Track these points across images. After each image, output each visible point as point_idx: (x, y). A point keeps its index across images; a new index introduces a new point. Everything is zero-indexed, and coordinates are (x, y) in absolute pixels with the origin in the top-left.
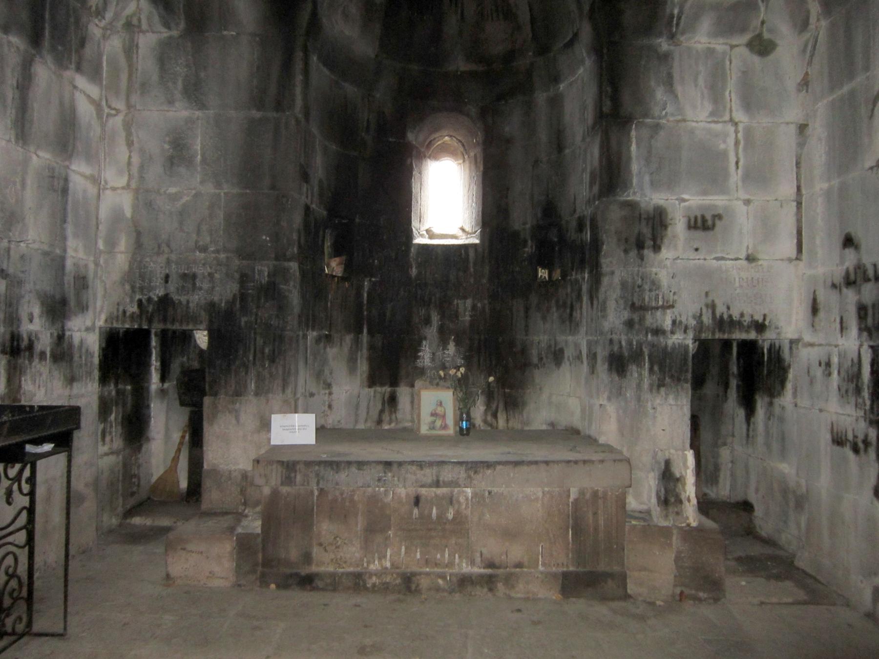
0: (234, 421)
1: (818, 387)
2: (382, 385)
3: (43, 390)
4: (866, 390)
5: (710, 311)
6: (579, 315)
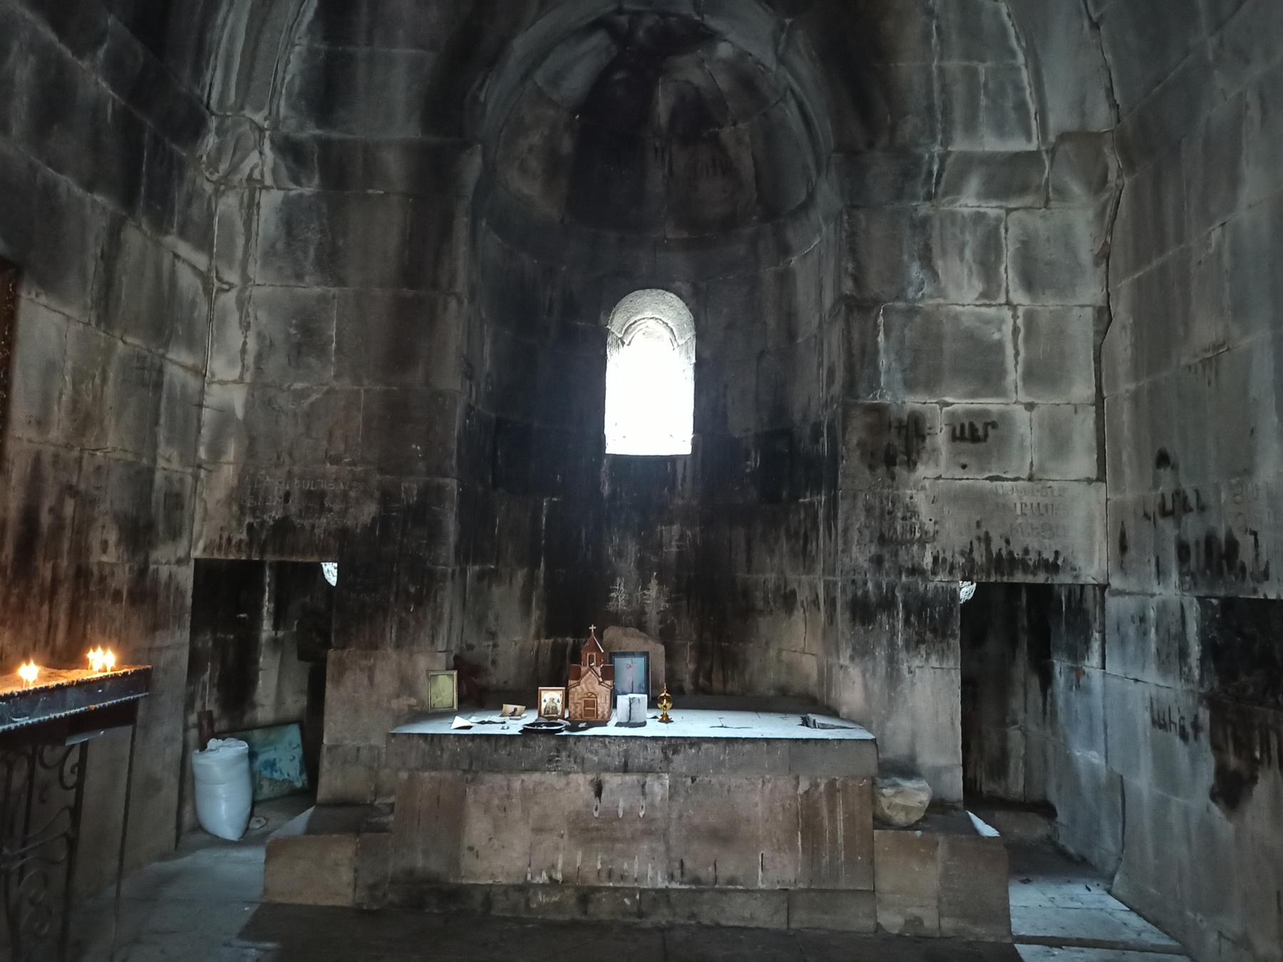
5: (983, 545)
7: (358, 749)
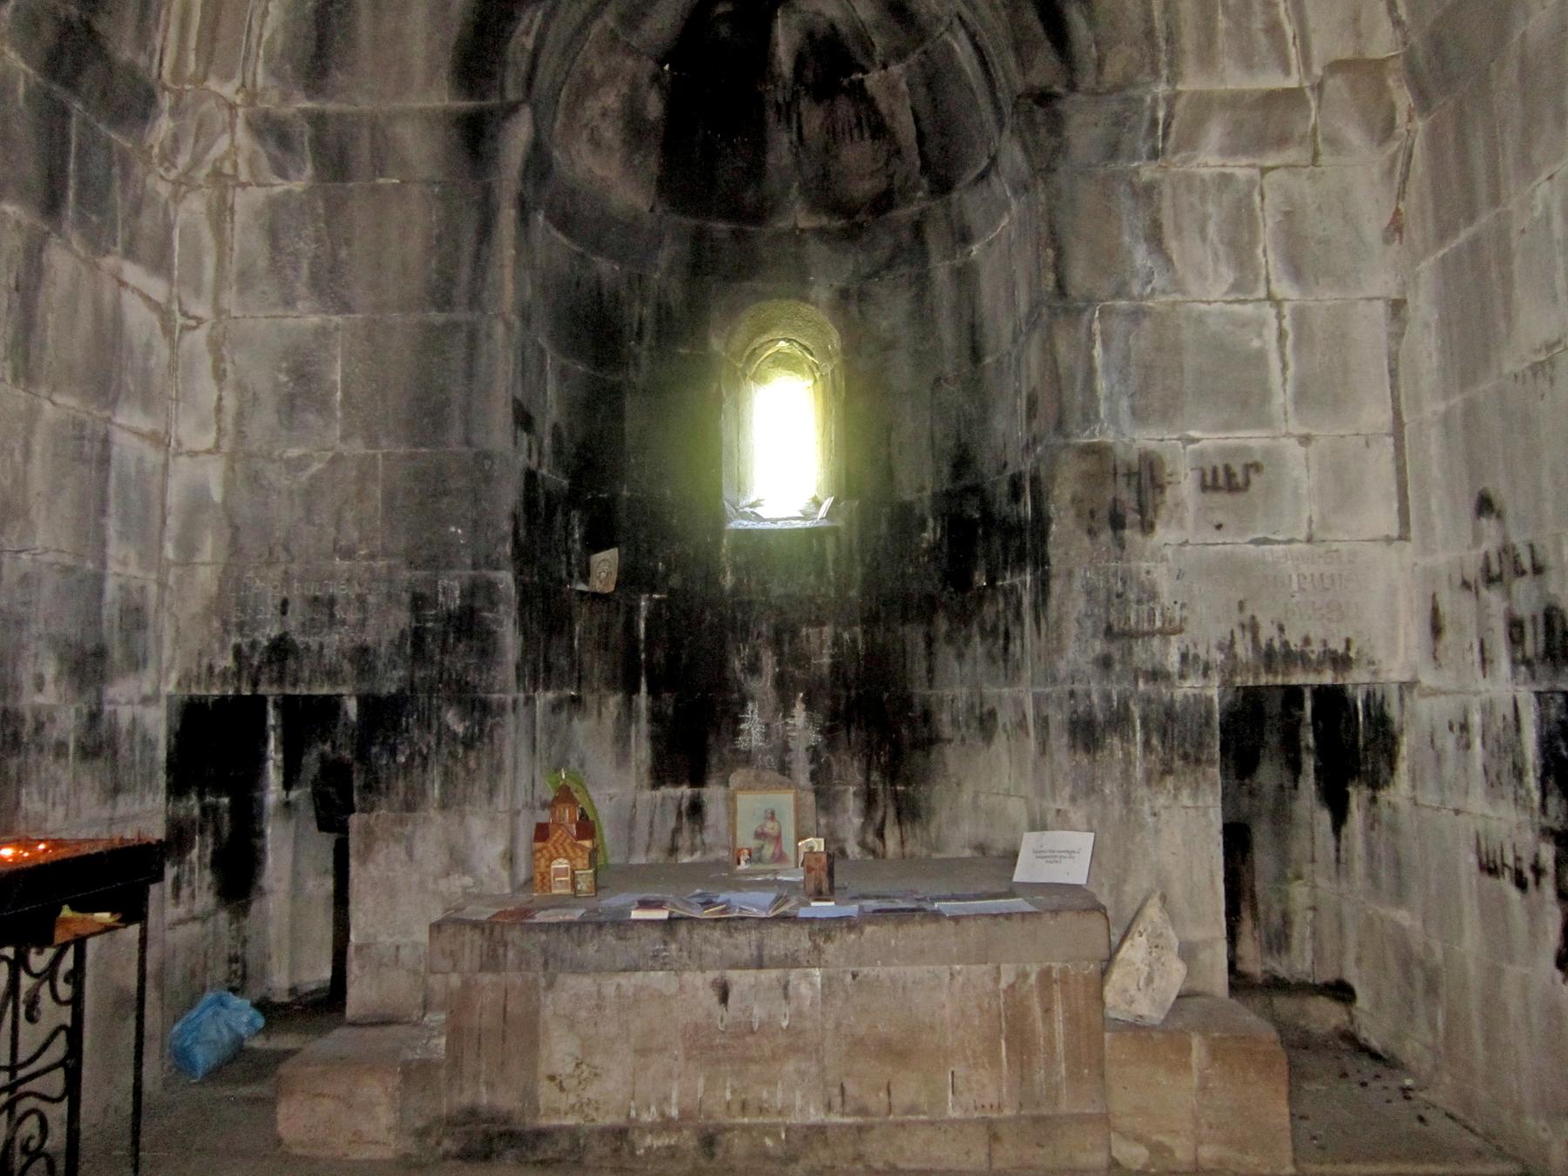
1: (1449, 770)
2: (677, 783)
3: (60, 811)
4: (1531, 774)
5: (1248, 636)
6: (1018, 649)
7: (398, 948)
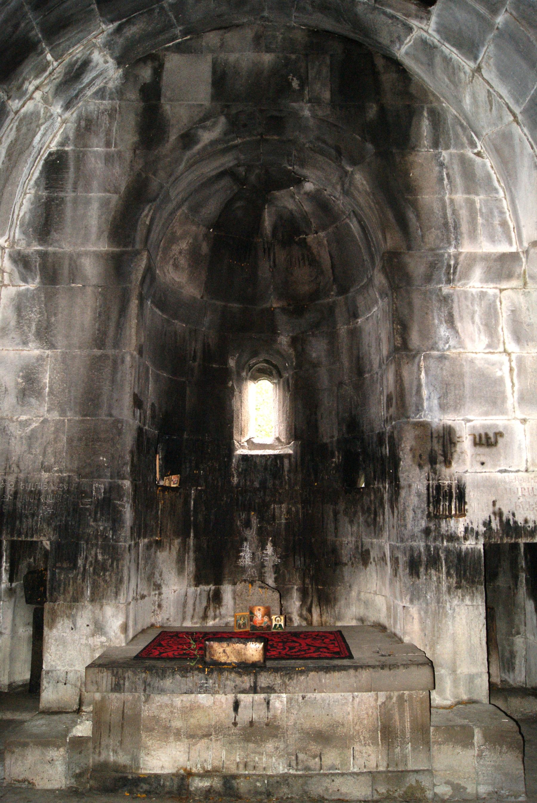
0: (71, 625)
2: (208, 583)
5: (498, 518)
6: (382, 520)
7: (67, 672)
